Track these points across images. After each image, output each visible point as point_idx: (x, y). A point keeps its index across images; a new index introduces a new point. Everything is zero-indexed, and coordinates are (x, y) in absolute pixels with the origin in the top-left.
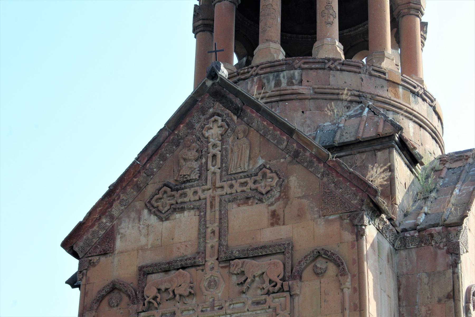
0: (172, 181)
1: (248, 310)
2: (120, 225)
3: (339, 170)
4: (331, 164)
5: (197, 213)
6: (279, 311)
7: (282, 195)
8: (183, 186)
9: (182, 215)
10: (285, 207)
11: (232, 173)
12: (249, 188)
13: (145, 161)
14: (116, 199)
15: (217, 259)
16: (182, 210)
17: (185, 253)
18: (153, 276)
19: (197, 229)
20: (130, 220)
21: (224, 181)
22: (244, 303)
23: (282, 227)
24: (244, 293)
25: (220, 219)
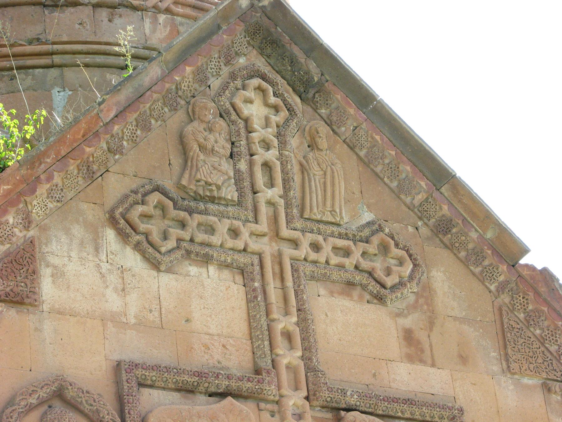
0: (168, 184)
2: (46, 245)
3: (543, 290)
4: (525, 273)
5: (239, 279)
7: (421, 301)
8: (202, 206)
9: (204, 270)
10: (431, 330)
11: (314, 217)
12: (355, 263)
13: (112, 114)
14: (43, 177)
15: (307, 398)
16: (206, 260)
17: (224, 363)
18: (155, 393)
19: (245, 316)
20: (71, 240)
23: (432, 370)
25: (299, 310)
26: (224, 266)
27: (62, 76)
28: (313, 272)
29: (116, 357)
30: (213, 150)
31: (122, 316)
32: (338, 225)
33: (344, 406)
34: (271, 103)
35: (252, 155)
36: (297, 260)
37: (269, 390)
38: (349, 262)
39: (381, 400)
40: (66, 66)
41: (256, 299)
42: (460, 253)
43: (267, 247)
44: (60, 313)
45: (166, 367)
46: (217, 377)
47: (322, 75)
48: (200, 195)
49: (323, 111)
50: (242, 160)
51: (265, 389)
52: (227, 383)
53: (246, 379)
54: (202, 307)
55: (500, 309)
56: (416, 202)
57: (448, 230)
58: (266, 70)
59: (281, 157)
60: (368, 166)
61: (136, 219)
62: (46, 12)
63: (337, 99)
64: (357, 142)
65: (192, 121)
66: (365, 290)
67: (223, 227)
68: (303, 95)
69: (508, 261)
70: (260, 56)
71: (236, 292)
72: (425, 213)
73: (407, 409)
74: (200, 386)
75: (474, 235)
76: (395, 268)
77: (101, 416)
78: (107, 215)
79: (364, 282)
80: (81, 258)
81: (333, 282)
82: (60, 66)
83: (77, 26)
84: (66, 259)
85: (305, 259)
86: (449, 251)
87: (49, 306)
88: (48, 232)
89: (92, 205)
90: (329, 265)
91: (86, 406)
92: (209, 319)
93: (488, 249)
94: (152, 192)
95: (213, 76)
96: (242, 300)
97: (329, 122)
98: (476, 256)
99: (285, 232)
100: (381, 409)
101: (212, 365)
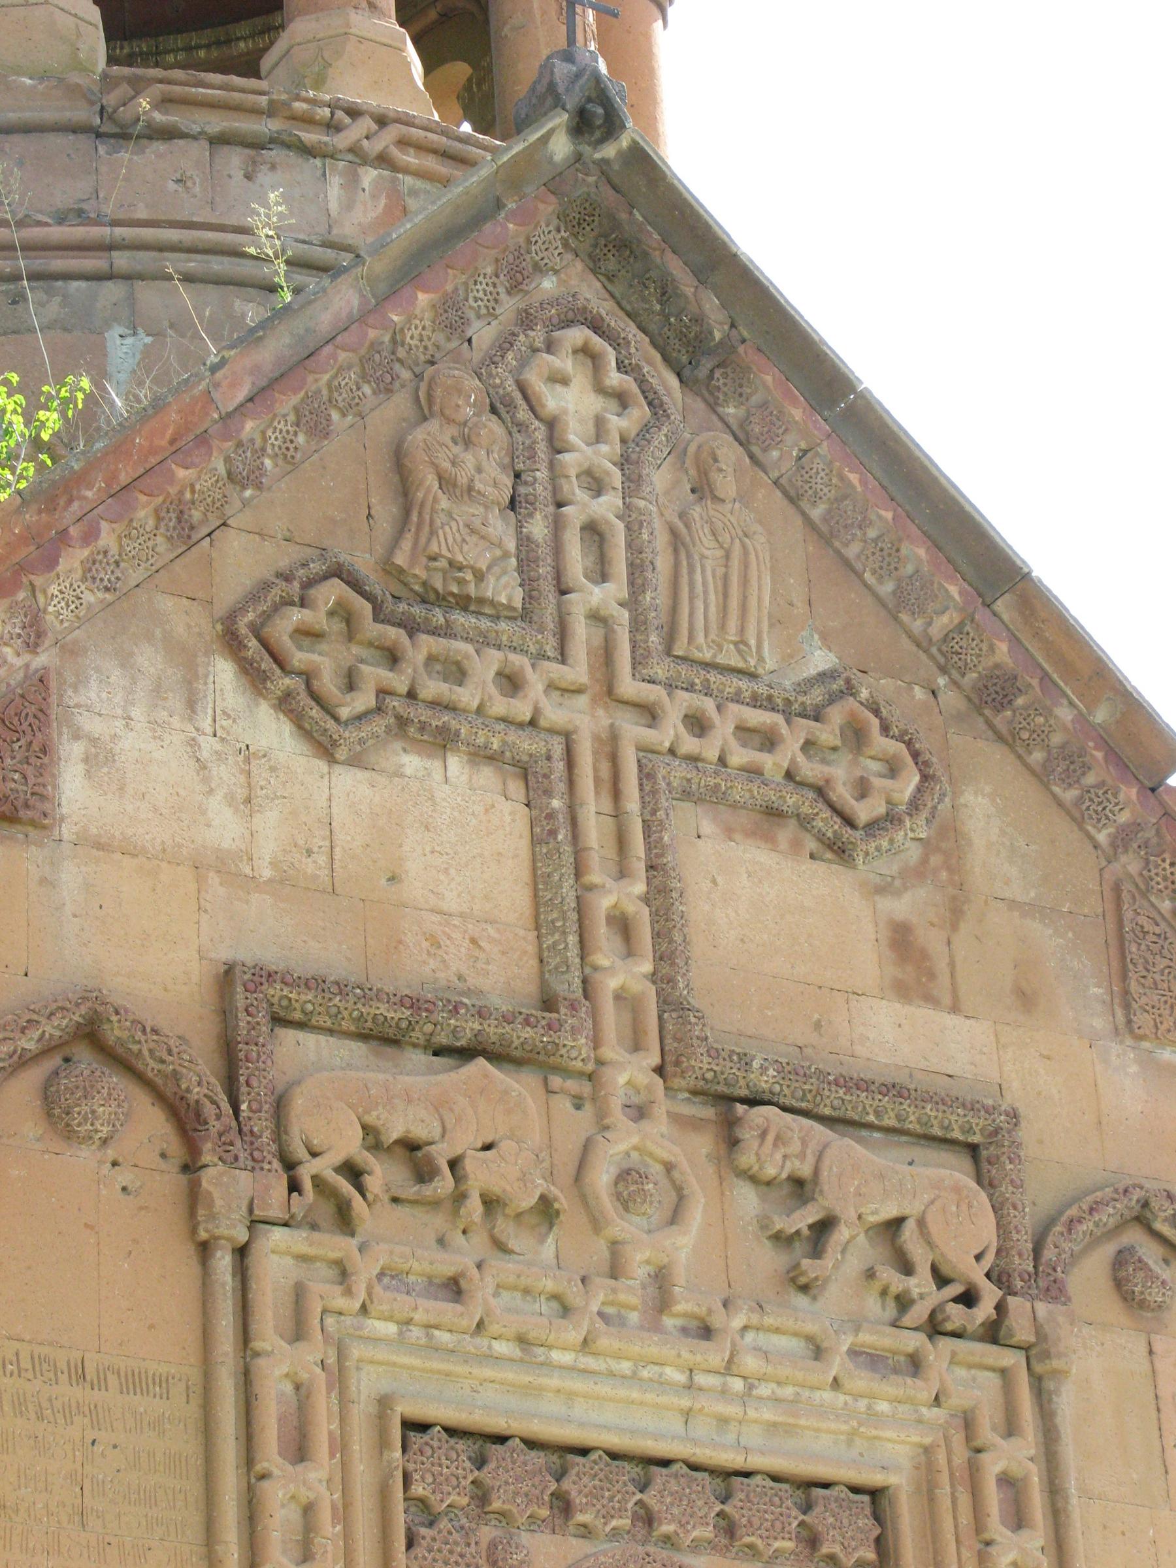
0: (364, 563)
1: (836, 1384)
2: (76, 691)
5: (516, 788)
6: (987, 1433)
7: (935, 860)
9: (435, 765)
10: (954, 927)
11: (697, 655)
12: (786, 765)
13: (241, 395)
14: (74, 531)
15: (660, 1070)
16: (442, 741)
17: (473, 981)
18: (310, 1041)
19: (526, 875)
21: (652, 681)
22: (810, 1339)
24: (805, 1289)
25: (651, 867)
26: (482, 756)
27: (131, 300)
28: (689, 781)
29: (225, 954)
30: (470, 489)
31: (241, 861)
32: (753, 676)
33: (744, 1092)
34: (612, 388)
35: (560, 505)
36: (653, 752)
37: (572, 1047)
38: (772, 764)
39: (829, 1083)
40: (141, 277)
41: (553, 838)
42: (1030, 753)
43: (583, 718)
44: (99, 846)
45: (337, 983)
46: (456, 1010)
47: (733, 326)
48: (436, 592)
49: (731, 410)
50: (538, 516)
51: (564, 1046)
52: (477, 1026)
53: (520, 1019)
54: (428, 849)
55: (1117, 889)
56: (936, 631)
57: (1005, 701)
58: (603, 307)
59: (627, 512)
60: (828, 543)
61: (286, 638)
62: (102, 150)
63: (764, 384)
64: (807, 487)
65: (425, 419)
66: (807, 830)
67: (485, 667)
68: (686, 372)
69: (1141, 777)
70: (591, 276)
71: (508, 819)
72: (956, 658)
73: (890, 1106)
74: (413, 1030)
75: (1065, 714)
76: (877, 782)
77: (184, 1086)
78: (219, 627)
79: (806, 809)
80: (153, 723)
81: (734, 806)
82: (128, 277)
83: (172, 186)
84: (120, 723)
85: (672, 752)
86: (1006, 749)
87: (75, 829)
88: (79, 660)
89: (185, 600)
90: (725, 765)
91: (151, 1062)
92: (442, 877)
93: (1096, 748)
94: (326, 577)
95: (479, 317)
96: (521, 837)
97: (742, 437)
98: (1066, 764)
99: (629, 686)
100: (828, 1102)
101: (443, 983)
